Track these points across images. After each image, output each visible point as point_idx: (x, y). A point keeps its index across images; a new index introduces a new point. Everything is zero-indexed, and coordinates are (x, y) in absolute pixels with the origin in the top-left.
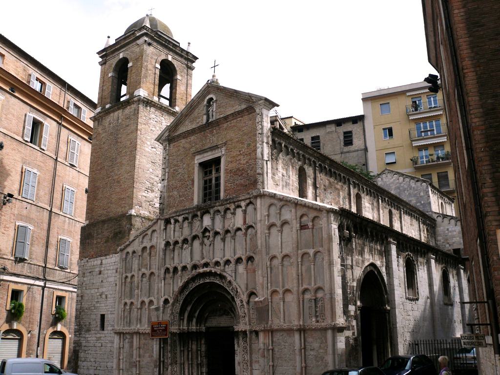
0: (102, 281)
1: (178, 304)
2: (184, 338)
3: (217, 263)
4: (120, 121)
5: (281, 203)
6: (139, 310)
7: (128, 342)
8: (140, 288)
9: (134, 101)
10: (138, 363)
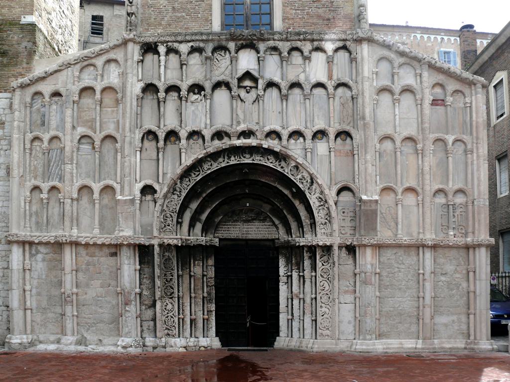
1: (176, 197)
2: (186, 254)
3: (273, 134)
5: (402, 60)
6: (75, 202)
7: (44, 260)
8: (75, 162)
10: (74, 297)
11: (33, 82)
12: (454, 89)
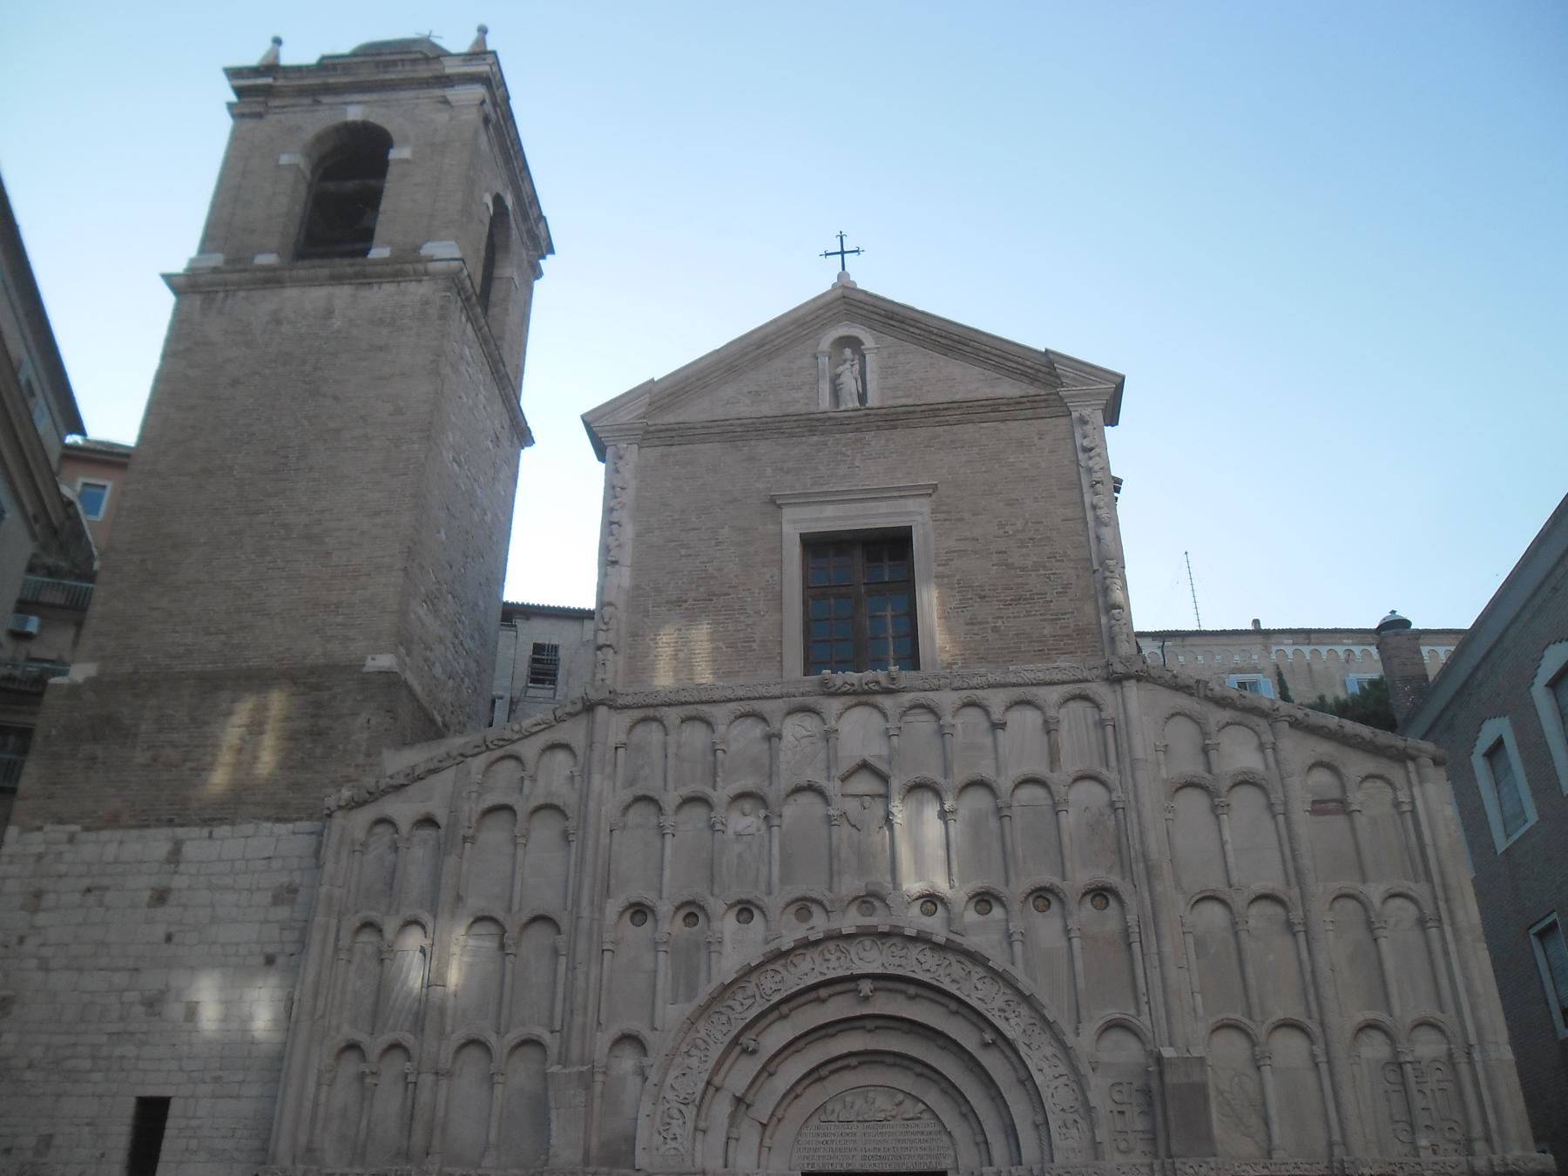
0: (169, 938)
4: (337, 323)
9: (426, 273)
11: (374, 796)
12: (1364, 774)
